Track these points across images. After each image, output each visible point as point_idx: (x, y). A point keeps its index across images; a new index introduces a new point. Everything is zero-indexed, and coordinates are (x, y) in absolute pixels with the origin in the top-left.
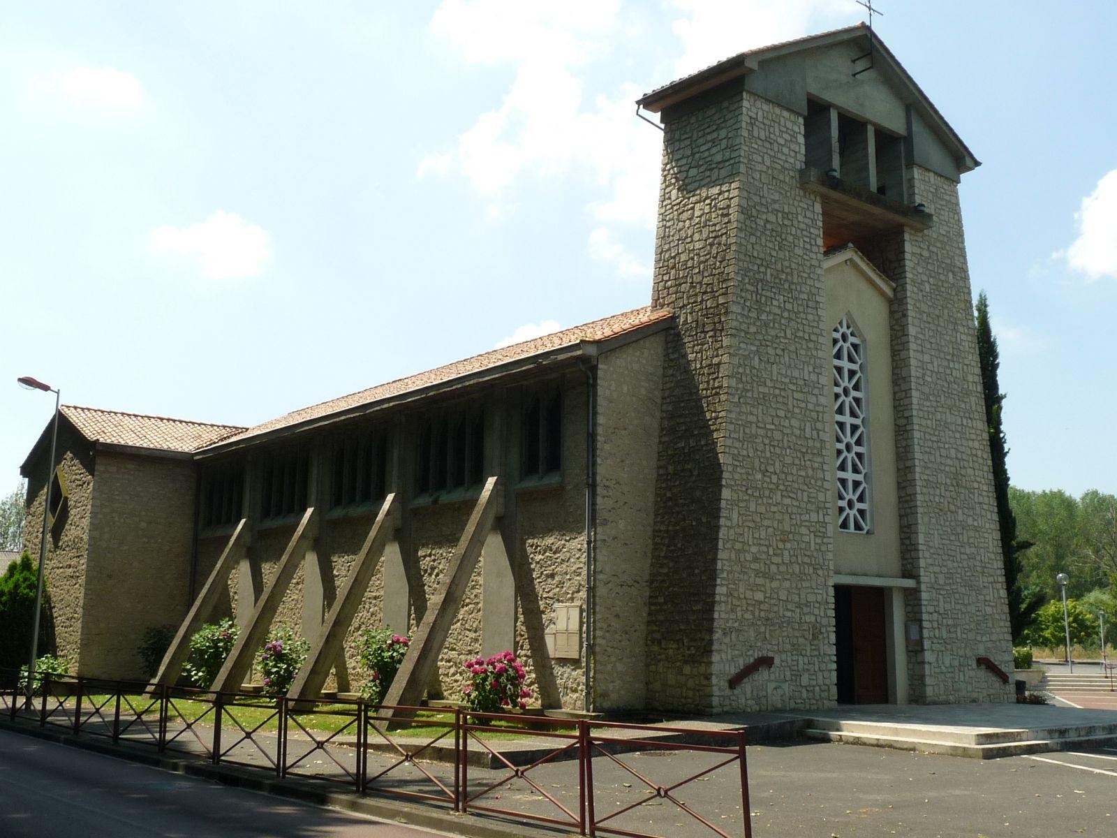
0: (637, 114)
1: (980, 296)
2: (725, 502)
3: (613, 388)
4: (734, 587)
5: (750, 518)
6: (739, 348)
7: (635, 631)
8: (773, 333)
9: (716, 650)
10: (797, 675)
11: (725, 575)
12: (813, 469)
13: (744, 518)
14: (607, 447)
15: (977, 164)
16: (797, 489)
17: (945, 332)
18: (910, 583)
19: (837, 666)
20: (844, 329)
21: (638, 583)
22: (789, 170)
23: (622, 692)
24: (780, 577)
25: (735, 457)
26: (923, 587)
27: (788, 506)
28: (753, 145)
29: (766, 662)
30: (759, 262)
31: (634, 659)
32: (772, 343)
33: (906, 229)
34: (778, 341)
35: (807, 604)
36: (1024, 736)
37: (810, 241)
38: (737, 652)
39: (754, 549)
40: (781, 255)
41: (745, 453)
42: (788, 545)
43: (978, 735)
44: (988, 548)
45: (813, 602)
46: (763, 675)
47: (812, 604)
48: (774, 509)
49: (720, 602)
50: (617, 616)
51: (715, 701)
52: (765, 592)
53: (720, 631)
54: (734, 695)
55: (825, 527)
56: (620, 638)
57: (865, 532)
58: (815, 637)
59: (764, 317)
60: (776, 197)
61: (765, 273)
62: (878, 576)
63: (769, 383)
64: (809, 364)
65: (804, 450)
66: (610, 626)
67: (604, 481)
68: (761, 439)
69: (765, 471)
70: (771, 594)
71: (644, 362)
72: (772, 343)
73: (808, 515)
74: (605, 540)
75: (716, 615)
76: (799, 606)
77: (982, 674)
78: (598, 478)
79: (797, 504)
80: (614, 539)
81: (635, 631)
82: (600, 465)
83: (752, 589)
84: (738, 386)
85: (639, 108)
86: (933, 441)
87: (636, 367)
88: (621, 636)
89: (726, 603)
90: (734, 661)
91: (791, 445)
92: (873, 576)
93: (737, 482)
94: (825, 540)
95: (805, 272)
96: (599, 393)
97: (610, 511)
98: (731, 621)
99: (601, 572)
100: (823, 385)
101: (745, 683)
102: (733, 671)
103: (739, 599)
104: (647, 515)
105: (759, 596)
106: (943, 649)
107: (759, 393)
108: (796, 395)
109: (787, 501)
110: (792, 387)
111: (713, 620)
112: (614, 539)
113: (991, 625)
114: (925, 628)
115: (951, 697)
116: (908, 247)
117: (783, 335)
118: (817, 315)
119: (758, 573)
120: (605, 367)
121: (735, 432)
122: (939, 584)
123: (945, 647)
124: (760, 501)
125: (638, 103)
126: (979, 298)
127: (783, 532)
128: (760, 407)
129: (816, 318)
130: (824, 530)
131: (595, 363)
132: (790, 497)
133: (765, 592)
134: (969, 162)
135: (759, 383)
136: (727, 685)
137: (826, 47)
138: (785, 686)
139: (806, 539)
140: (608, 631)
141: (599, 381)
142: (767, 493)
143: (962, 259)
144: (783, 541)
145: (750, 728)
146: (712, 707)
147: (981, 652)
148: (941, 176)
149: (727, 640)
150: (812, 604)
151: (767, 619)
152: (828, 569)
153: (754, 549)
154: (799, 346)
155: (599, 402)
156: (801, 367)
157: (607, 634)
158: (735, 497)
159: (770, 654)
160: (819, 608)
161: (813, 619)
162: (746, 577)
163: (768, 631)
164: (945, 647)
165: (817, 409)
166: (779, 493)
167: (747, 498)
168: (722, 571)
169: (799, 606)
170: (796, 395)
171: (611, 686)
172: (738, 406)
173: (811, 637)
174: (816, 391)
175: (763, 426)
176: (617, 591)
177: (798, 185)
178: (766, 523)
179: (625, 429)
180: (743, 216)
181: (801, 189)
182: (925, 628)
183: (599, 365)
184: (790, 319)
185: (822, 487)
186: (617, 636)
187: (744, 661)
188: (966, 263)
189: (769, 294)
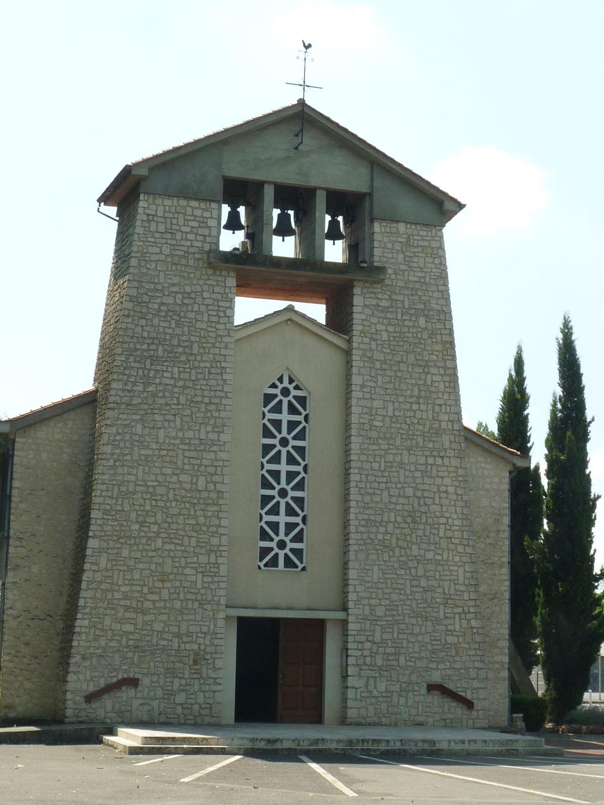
0: (98, 211)
1: (565, 318)
2: (91, 550)
3: (31, 456)
4: (98, 620)
5: (122, 562)
6: (118, 419)
7: (46, 656)
8: (162, 401)
9: (73, 672)
10: (171, 693)
11: (88, 610)
12: (206, 517)
13: (114, 563)
14: (22, 506)
15: (461, 206)
16: (183, 536)
17: (409, 376)
18: (340, 615)
19: (583, 694)
20: (286, 383)
21: (52, 617)
22: (195, 253)
23: (30, 705)
24: (155, 612)
25: (106, 512)
26: (351, 619)
27: (169, 551)
28: (149, 239)
29: (133, 682)
30: (149, 341)
31: (43, 680)
32: (160, 409)
33: (355, 283)
34: (168, 408)
35: (189, 634)
36: (213, 742)
37: (217, 314)
38: (96, 674)
39: (124, 589)
40: (178, 331)
41: (119, 508)
42: (168, 585)
43: (146, 738)
44: (457, 580)
45: (197, 633)
46: (127, 693)
47: (195, 634)
48: (151, 554)
49: (79, 633)
50: (27, 644)
51: (69, 712)
52: (135, 625)
53: (79, 657)
54: (90, 708)
55: (218, 568)
56: (29, 662)
57: (300, 569)
58: (196, 662)
59: (151, 388)
60: (176, 280)
61: (157, 350)
62: (308, 609)
63: (154, 446)
64: (206, 424)
65: (195, 501)
66: (18, 651)
67: (18, 534)
68: (141, 495)
69: (142, 524)
70: (143, 625)
71: (68, 431)
72: (160, 409)
73: (196, 558)
74: (16, 582)
75: (75, 643)
76: (178, 635)
77: (436, 699)
78: (11, 532)
79: (183, 548)
80: (26, 581)
81: (46, 656)
82: (13, 521)
83: (120, 623)
84: (114, 451)
85: (100, 206)
86: (379, 483)
87: (57, 436)
88: (30, 660)
89: (87, 634)
90: (93, 681)
91: (178, 497)
92: (302, 610)
93: (108, 533)
94: (216, 579)
95: (209, 343)
96: (15, 462)
97: (22, 558)
98: (92, 648)
99: (11, 608)
100: (224, 442)
101: (105, 699)
102: (92, 688)
103: (103, 630)
104: (64, 560)
105: (129, 628)
106: (377, 675)
107: (140, 455)
108: (187, 454)
109: (167, 547)
110: (183, 447)
111: (71, 647)
112: (26, 581)
113: (453, 653)
114: (351, 656)
115: (383, 719)
116: (358, 300)
117: (176, 402)
118: (222, 379)
119: (127, 608)
120: (23, 440)
121: (107, 491)
122: (376, 616)
123: (380, 673)
124: (135, 548)
125: (100, 200)
126: (563, 321)
127: (163, 573)
128: (141, 467)
129: (221, 383)
130: (216, 570)
131: (13, 437)
132: (174, 543)
133: (135, 625)
134: (448, 205)
135: (140, 447)
136: (83, 699)
137: (258, 130)
138: (155, 704)
139: (193, 578)
140: (16, 656)
141: (15, 452)
142: (144, 541)
143: (442, 302)
144: (163, 581)
145: (43, 731)
146: (66, 717)
147: (436, 678)
148: (416, 224)
149: (87, 663)
150: (195, 634)
151: (137, 647)
152: (218, 604)
153: (124, 589)
154: (194, 410)
155: (14, 470)
156: (197, 428)
157: (15, 659)
158: (105, 545)
159: (137, 676)
160: (204, 638)
161: (195, 647)
162: (113, 612)
163: (136, 657)
164: (380, 673)
165: (215, 464)
166: (160, 540)
167: (119, 546)
168: (85, 607)
169: (178, 635)
170: (187, 454)
171: (17, 700)
172: (113, 469)
173: (191, 662)
174: (215, 448)
175: (143, 483)
176: (28, 623)
177: (205, 266)
178: (141, 566)
179: (43, 490)
180: (132, 304)
181: (209, 268)
182: (351, 656)
183: (17, 439)
184: (185, 387)
185: (217, 532)
186: (26, 661)
187: (105, 680)
188: (448, 303)
189: (159, 368)
